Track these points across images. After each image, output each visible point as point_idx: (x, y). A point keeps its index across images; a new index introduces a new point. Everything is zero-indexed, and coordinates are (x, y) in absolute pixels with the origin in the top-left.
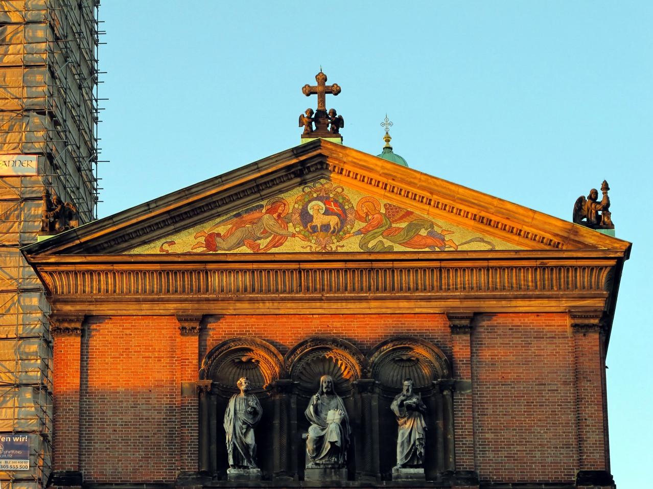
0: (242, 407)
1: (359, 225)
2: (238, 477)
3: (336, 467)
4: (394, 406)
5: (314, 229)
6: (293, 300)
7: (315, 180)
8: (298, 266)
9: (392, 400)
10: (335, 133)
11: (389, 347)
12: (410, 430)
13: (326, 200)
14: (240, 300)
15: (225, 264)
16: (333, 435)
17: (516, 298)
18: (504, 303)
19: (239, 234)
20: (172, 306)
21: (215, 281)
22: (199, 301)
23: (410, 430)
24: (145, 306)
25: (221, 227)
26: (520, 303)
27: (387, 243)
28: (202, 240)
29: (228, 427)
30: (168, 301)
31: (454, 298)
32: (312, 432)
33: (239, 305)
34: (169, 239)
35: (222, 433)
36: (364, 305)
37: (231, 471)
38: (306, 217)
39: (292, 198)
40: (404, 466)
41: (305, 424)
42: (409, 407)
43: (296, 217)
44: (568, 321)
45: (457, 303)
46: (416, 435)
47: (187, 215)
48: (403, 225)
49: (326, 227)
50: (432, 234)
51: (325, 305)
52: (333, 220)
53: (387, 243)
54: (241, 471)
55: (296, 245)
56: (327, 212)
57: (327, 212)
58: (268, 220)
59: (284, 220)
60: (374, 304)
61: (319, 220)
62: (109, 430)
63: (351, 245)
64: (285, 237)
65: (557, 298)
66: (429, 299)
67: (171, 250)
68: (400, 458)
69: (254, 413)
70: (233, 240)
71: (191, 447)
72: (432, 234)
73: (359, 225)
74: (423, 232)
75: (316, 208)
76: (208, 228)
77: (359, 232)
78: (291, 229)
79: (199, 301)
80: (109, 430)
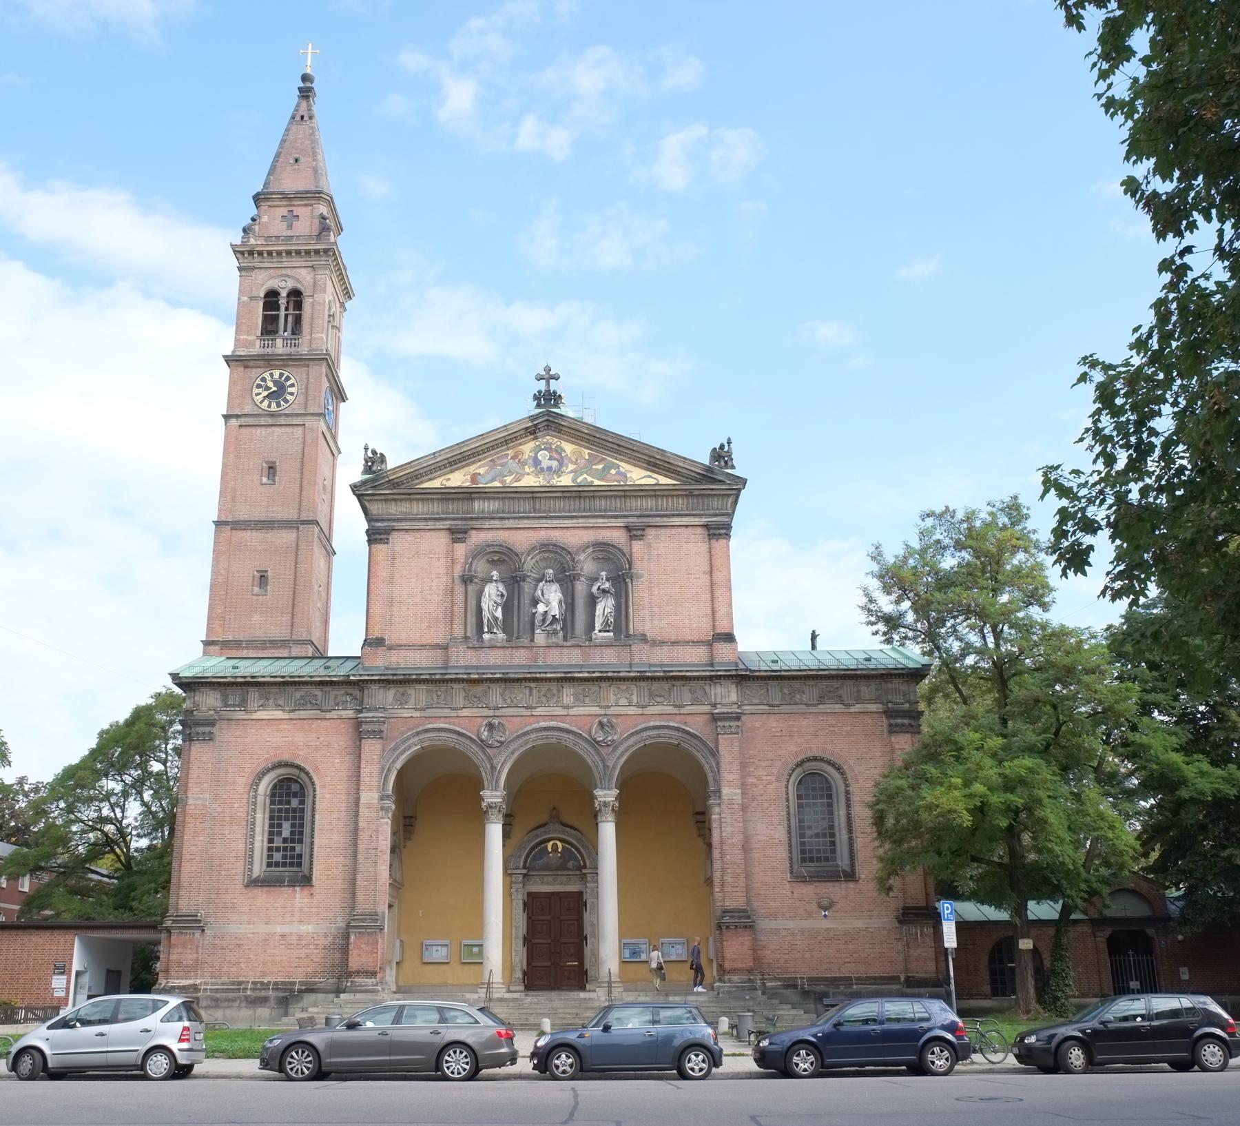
2: (491, 640)
5: (542, 469)
6: (528, 518)
8: (532, 495)
11: (591, 550)
12: (605, 607)
13: (549, 449)
14: (493, 518)
15: (484, 494)
16: (555, 610)
17: (673, 516)
19: (493, 473)
20: (448, 523)
21: (477, 505)
22: (466, 519)
23: (605, 607)
24: (430, 523)
25: (480, 468)
26: (675, 519)
27: (590, 479)
28: (468, 477)
29: (484, 606)
30: (446, 519)
32: (541, 608)
34: (447, 477)
37: (486, 636)
38: (536, 462)
39: (528, 448)
41: (535, 602)
42: (604, 591)
43: (531, 461)
45: (635, 520)
47: (460, 461)
48: (600, 467)
49: (550, 468)
50: (618, 473)
52: (555, 464)
53: (590, 479)
54: (493, 636)
55: (530, 480)
56: (551, 459)
57: (551, 459)
58: (512, 464)
59: (523, 464)
60: (581, 520)
61: (545, 464)
62: (404, 608)
63: (566, 480)
64: (523, 475)
65: (700, 516)
66: (616, 517)
67: (449, 484)
68: (598, 626)
70: (489, 477)
71: (458, 620)
72: (618, 473)
73: (571, 467)
74: (613, 472)
75: (543, 455)
76: (472, 469)
77: (571, 472)
78: (527, 469)
79: (466, 519)
80: (404, 608)
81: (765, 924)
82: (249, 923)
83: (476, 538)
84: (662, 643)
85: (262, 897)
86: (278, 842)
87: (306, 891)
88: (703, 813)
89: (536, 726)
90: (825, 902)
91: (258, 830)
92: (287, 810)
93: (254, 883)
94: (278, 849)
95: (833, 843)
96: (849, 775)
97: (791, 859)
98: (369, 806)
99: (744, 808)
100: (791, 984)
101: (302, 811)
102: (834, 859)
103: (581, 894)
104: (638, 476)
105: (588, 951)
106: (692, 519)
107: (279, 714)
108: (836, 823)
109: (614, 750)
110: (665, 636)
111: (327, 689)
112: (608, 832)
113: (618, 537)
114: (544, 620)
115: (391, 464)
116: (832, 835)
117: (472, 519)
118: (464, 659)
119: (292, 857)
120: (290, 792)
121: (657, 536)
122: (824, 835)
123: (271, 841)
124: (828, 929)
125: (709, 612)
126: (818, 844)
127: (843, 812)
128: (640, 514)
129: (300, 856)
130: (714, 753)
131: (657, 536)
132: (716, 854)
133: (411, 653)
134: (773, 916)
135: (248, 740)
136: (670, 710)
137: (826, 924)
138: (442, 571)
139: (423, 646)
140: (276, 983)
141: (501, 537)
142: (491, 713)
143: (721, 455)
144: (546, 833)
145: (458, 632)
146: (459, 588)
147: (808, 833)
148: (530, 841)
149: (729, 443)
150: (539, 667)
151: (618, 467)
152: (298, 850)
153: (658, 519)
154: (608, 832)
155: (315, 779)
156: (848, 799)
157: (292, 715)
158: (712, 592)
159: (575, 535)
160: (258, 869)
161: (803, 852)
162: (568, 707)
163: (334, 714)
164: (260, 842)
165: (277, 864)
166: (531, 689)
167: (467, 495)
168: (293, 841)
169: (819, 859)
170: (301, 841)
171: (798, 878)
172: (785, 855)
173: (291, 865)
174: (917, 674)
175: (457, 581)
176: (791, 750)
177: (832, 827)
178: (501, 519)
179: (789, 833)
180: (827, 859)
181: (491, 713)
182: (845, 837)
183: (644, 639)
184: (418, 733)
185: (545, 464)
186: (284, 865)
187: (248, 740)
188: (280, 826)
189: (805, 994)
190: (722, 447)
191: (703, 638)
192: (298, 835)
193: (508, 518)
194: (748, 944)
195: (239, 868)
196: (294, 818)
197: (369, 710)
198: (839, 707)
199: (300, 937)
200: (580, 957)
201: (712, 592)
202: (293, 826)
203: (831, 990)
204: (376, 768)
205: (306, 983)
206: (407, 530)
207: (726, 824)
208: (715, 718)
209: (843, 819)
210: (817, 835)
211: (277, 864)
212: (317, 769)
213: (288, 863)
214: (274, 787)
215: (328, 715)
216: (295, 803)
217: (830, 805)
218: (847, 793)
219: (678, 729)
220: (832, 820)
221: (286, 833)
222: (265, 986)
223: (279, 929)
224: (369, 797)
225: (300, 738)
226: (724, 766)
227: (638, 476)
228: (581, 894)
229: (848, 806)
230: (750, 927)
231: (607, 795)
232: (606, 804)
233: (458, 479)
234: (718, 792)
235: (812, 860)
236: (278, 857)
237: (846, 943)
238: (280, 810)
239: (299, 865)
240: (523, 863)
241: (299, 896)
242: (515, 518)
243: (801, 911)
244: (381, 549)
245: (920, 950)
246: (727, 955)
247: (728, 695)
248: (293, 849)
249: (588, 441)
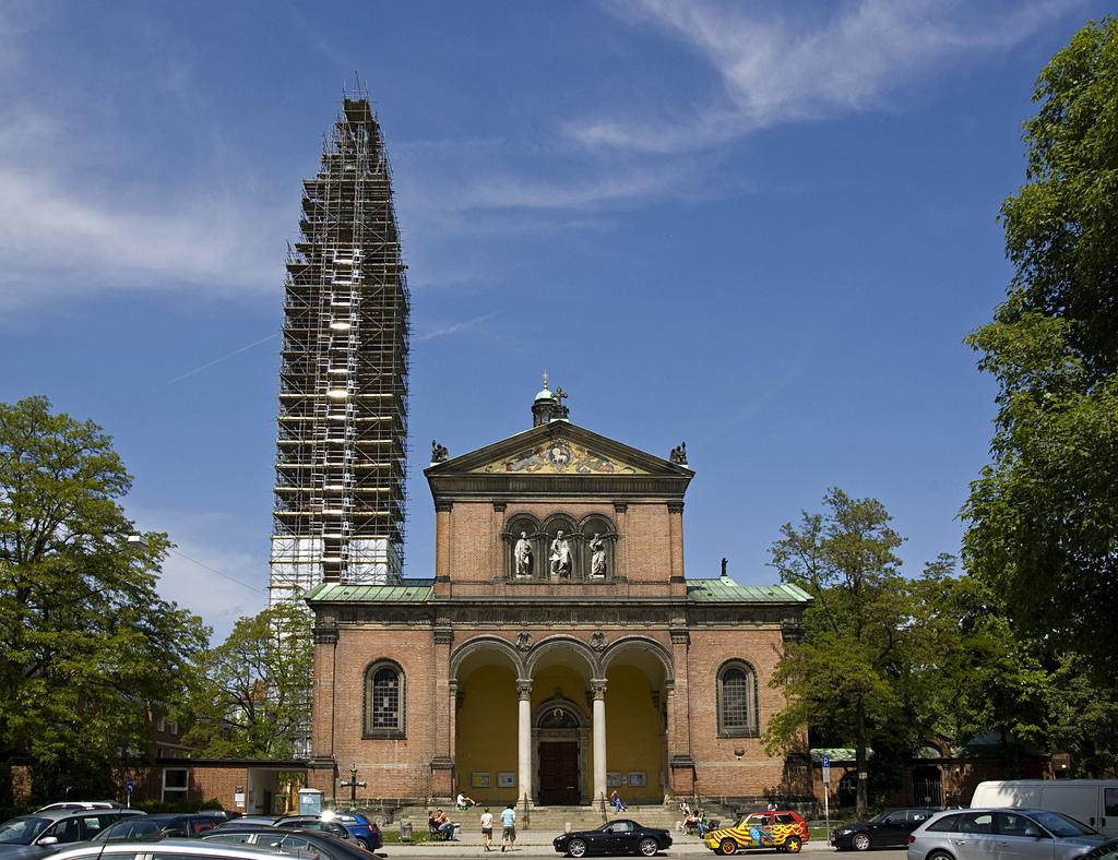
0: (523, 546)
1: (576, 460)
3: (565, 575)
4: (591, 545)
6: (546, 496)
8: (549, 479)
9: (589, 543)
10: (566, 417)
17: (645, 496)
29: (517, 555)
32: (555, 558)
35: (513, 557)
38: (552, 456)
43: (547, 456)
44: (666, 506)
46: (600, 560)
49: (561, 461)
52: (564, 458)
55: (547, 470)
57: (561, 454)
61: (558, 457)
63: (571, 470)
66: (606, 496)
68: (593, 571)
69: (528, 549)
70: (519, 466)
73: (576, 460)
81: (699, 765)
82: (365, 762)
83: (512, 509)
84: (637, 583)
85: (373, 745)
86: (381, 710)
87: (402, 742)
88: (658, 692)
89: (552, 637)
90: (739, 751)
92: (386, 690)
93: (366, 737)
94: (381, 715)
95: (745, 713)
96: (757, 670)
97: (718, 723)
98: (442, 688)
99: (688, 691)
100: (717, 801)
101: (397, 690)
102: (746, 724)
103: (576, 743)
104: (620, 469)
105: (581, 780)
107: (379, 626)
108: (747, 701)
109: (604, 654)
110: (639, 578)
111: (411, 610)
112: (599, 706)
113: (608, 510)
114: (558, 567)
115: (449, 457)
116: (745, 708)
117: (508, 495)
118: (503, 592)
119: (391, 720)
120: (384, 674)
121: (634, 510)
122: (740, 708)
123: (376, 709)
125: (669, 561)
126: (735, 714)
127: (752, 694)
128: (624, 492)
129: (396, 720)
130: (670, 656)
131: (634, 510)
132: (671, 720)
133: (467, 587)
134: (706, 759)
135: (359, 643)
136: (642, 627)
137: (739, 764)
138: (488, 531)
139: (476, 583)
140: (384, 800)
141: (528, 507)
142: (522, 628)
143: (679, 454)
144: (553, 704)
145: (500, 573)
147: (729, 706)
148: (542, 709)
149: (684, 446)
150: (554, 597)
151: (608, 461)
152: (394, 716)
154: (599, 706)
155: (405, 670)
156: (756, 686)
158: (671, 548)
159: (578, 508)
161: (726, 719)
163: (417, 627)
164: (370, 708)
165: (381, 725)
166: (549, 612)
167: (506, 478)
168: (391, 710)
169: (736, 724)
170: (396, 710)
171: (722, 736)
172: (715, 721)
173: (390, 725)
174: (802, 606)
176: (720, 656)
177: (744, 703)
178: (528, 496)
179: (718, 706)
180: (741, 723)
181: (522, 628)
182: (753, 710)
183: (625, 580)
184: (474, 641)
185: (558, 457)
186: (386, 725)
187: (359, 643)
188: (382, 700)
189: (725, 807)
190: (679, 449)
191: (664, 580)
192: (394, 706)
194: (691, 776)
195: (358, 726)
196: (391, 695)
197: (441, 625)
198: (753, 627)
199: (399, 772)
200: (576, 784)
201: (671, 548)
202: (390, 700)
204: (446, 663)
205: (405, 800)
207: (675, 703)
208: (672, 633)
209: (752, 698)
210: (735, 708)
211: (381, 725)
212: (406, 663)
213: (384, 724)
214: (377, 674)
215: (412, 628)
216: (391, 685)
217: (744, 689)
218: (756, 681)
219: (646, 640)
220: (744, 699)
221: (386, 705)
222: (378, 802)
223: (385, 766)
224: (443, 682)
225: (394, 643)
226: (677, 664)
227: (620, 469)
228: (576, 743)
229: (756, 690)
230: (693, 767)
231: (600, 681)
232: (600, 689)
233: (498, 468)
234: (672, 682)
235: (731, 724)
236: (381, 720)
238: (381, 690)
239: (396, 725)
240: (538, 724)
241: (397, 746)
243: (724, 756)
244: (445, 515)
246: (677, 783)
247: (679, 622)
248: (391, 715)
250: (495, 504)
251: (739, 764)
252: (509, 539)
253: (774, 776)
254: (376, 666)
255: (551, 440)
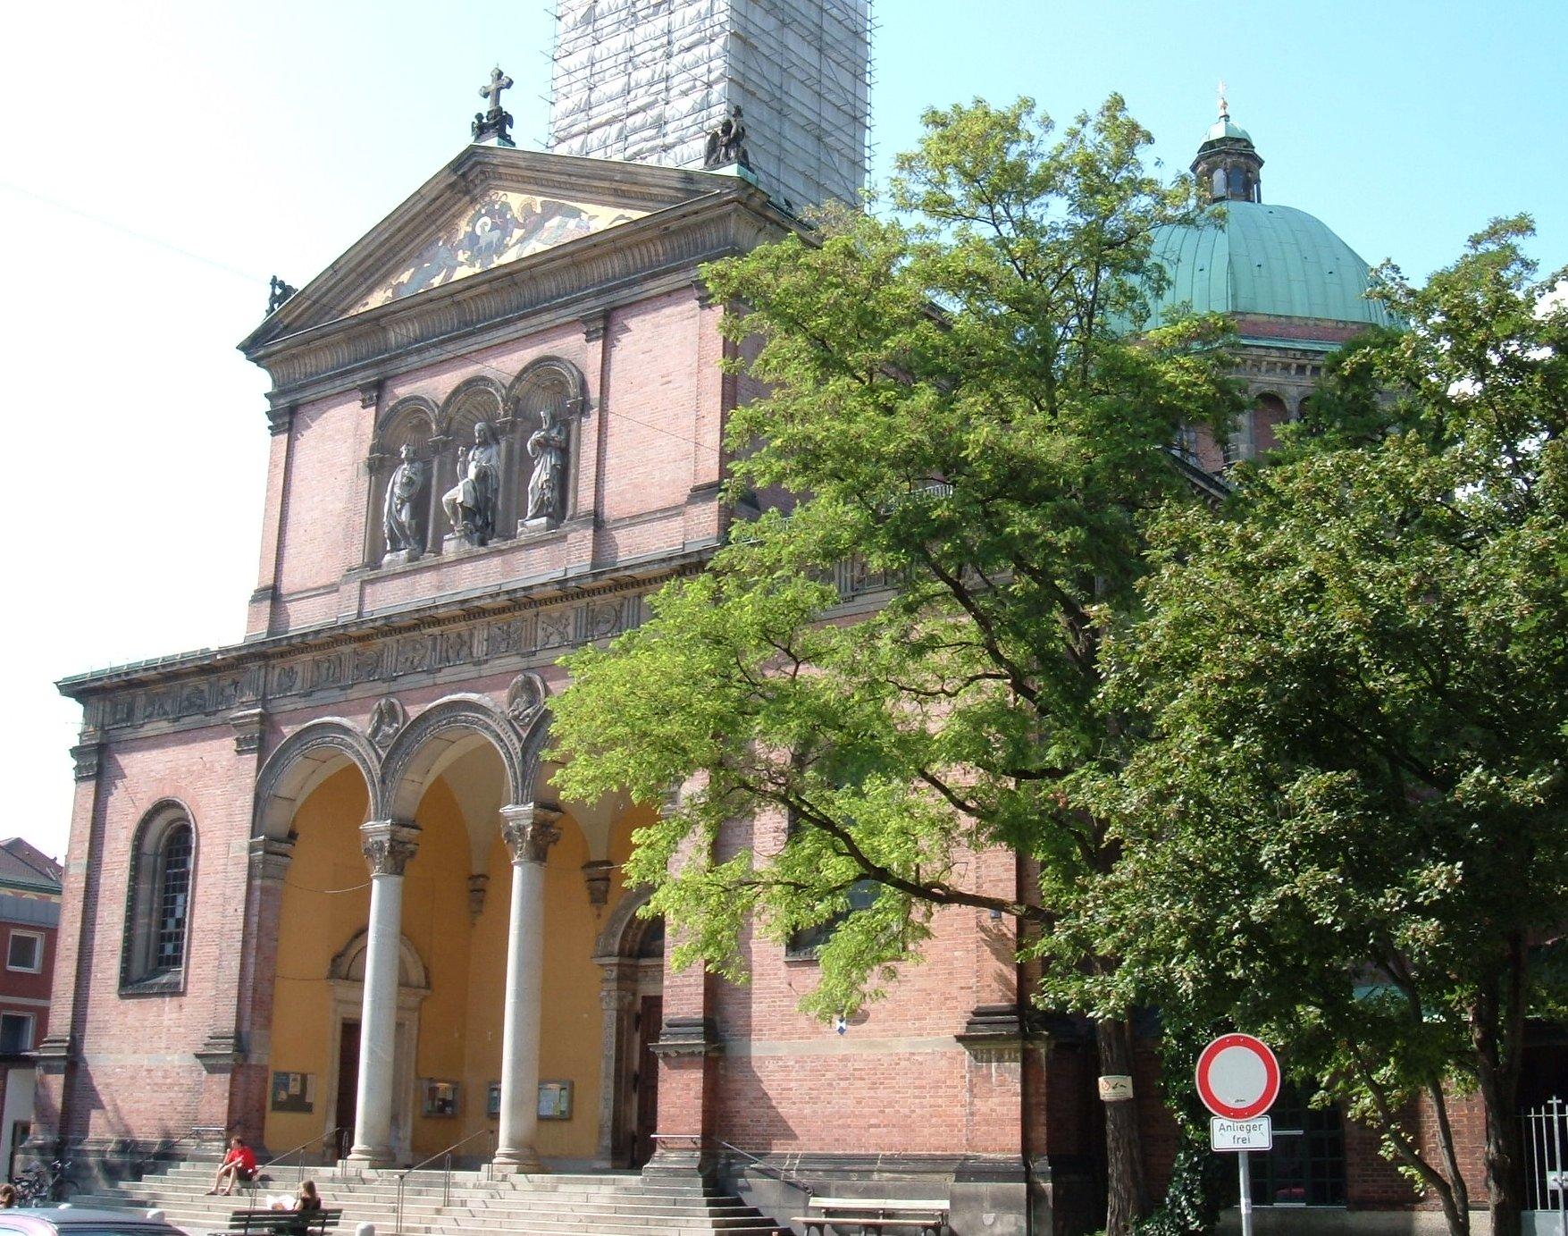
7: (483, 195)
12: (541, 474)
17: (645, 279)
18: (636, 289)
23: (541, 474)
26: (651, 284)
31: (587, 296)
33: (410, 360)
36: (512, 328)
40: (534, 517)
49: (490, 245)
51: (479, 339)
60: (521, 325)
91: (142, 908)
106: (674, 278)
124: (845, 1059)
146: (364, 483)
153: (625, 292)
157: (178, 726)
160: (137, 969)
162: (478, 663)
175: (363, 469)
178: (419, 351)
193: (427, 349)
203: (835, 1182)
206: (312, 402)
237: (873, 1086)
242: (434, 346)
245: (994, 1101)
249: (537, 182)
250: (363, 389)
251: (842, 1046)
252: (380, 465)
253: (937, 1086)
254: (159, 823)
255: (473, 201)
